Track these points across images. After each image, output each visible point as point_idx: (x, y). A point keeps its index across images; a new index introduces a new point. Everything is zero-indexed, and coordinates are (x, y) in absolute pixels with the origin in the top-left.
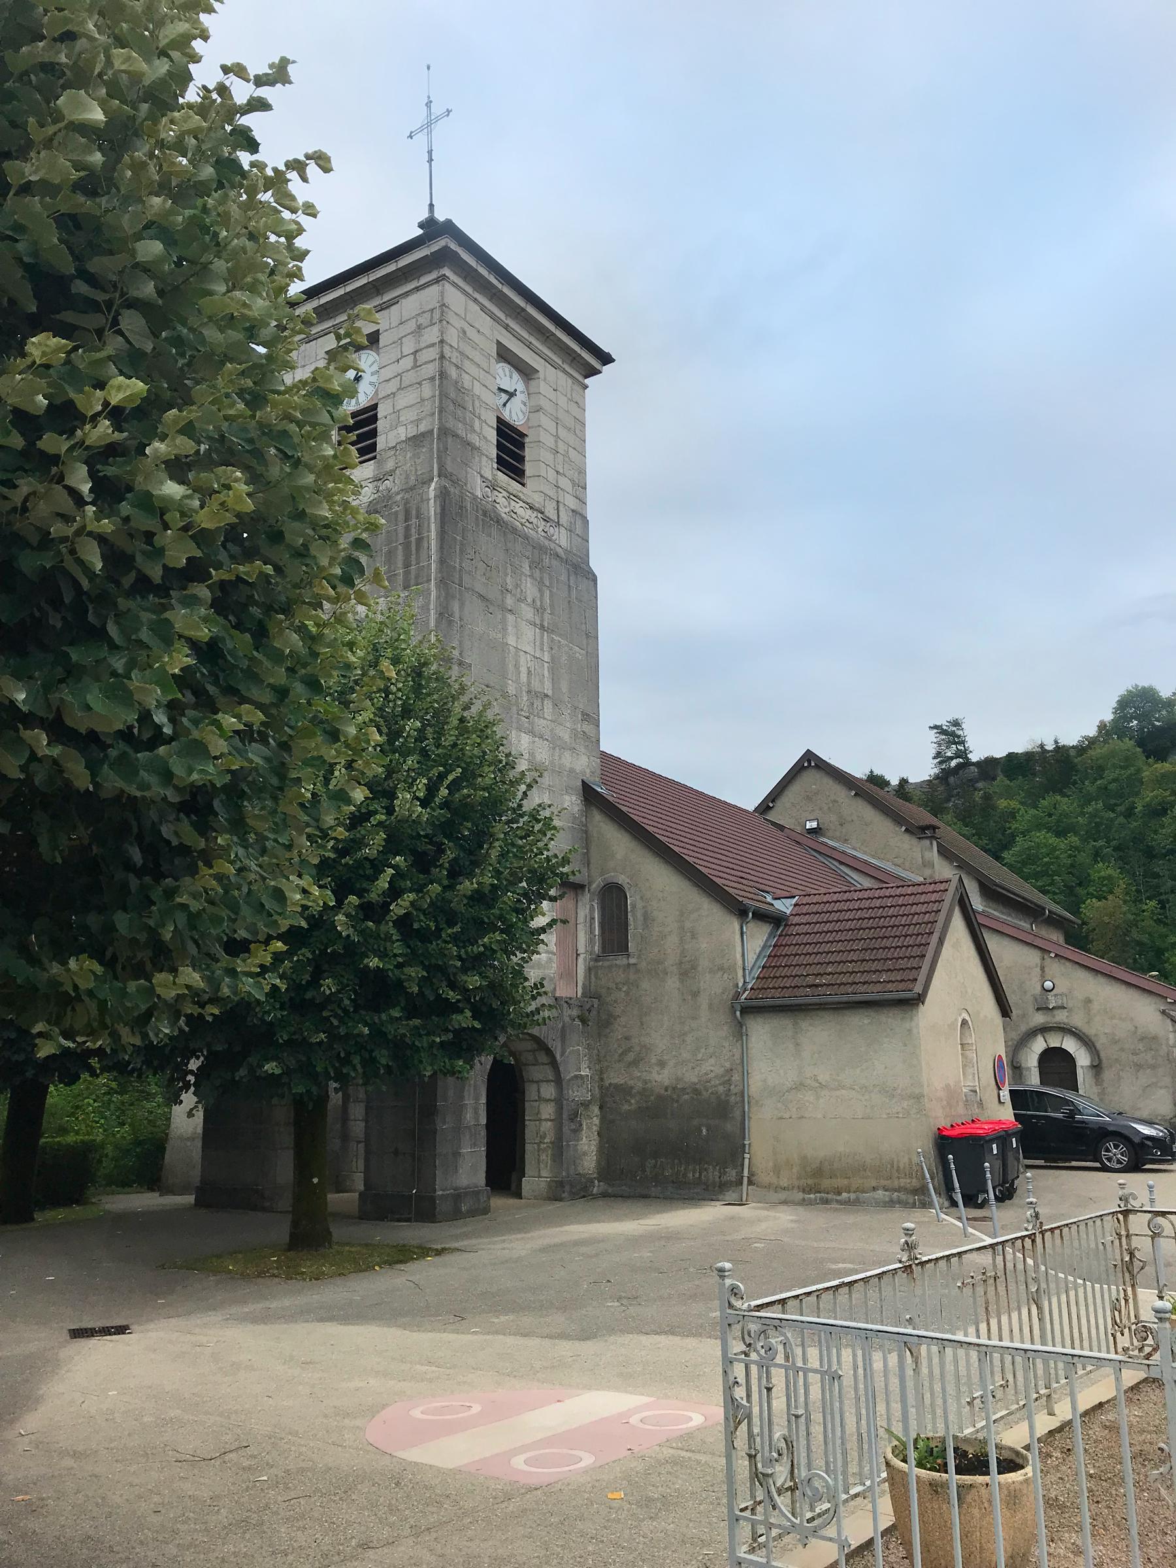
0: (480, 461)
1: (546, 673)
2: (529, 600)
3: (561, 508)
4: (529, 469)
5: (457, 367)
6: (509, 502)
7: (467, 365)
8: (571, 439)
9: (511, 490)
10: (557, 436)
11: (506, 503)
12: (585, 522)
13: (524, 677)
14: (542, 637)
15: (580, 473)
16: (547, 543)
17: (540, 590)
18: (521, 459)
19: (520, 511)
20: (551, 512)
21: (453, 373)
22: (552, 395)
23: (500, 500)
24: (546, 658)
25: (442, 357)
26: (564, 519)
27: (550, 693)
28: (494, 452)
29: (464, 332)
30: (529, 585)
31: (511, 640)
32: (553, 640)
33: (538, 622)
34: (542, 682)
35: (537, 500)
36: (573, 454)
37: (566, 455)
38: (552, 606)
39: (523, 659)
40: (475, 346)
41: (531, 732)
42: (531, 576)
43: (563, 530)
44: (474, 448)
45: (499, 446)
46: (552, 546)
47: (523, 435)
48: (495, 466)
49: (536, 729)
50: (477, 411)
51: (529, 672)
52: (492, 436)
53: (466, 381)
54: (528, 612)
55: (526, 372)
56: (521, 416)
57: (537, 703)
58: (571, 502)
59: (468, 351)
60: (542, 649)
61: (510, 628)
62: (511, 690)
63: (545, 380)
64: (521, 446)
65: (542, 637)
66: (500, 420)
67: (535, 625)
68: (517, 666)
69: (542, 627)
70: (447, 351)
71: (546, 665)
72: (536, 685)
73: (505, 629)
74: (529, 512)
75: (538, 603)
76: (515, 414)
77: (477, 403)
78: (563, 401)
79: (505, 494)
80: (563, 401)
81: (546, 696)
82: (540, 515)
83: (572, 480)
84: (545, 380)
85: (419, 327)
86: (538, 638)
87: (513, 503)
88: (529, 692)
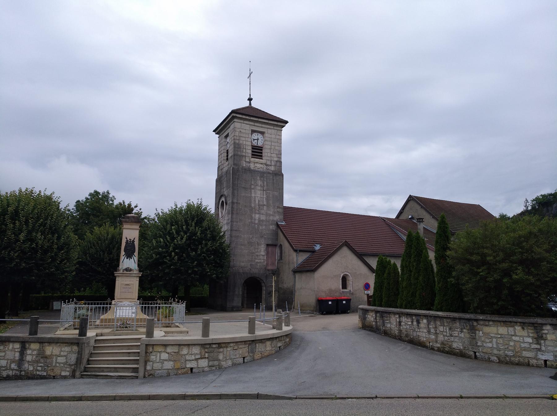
7: (242, 138)
8: (276, 144)
13: (257, 202)
20: (269, 163)
21: (237, 141)
24: (265, 196)
42: (260, 180)
44: (243, 156)
53: (241, 142)
54: (259, 188)
55: (262, 133)
57: (261, 207)
58: (276, 159)
59: (242, 135)
62: (253, 205)
68: (255, 201)
69: (264, 190)
70: (235, 137)
73: (251, 193)
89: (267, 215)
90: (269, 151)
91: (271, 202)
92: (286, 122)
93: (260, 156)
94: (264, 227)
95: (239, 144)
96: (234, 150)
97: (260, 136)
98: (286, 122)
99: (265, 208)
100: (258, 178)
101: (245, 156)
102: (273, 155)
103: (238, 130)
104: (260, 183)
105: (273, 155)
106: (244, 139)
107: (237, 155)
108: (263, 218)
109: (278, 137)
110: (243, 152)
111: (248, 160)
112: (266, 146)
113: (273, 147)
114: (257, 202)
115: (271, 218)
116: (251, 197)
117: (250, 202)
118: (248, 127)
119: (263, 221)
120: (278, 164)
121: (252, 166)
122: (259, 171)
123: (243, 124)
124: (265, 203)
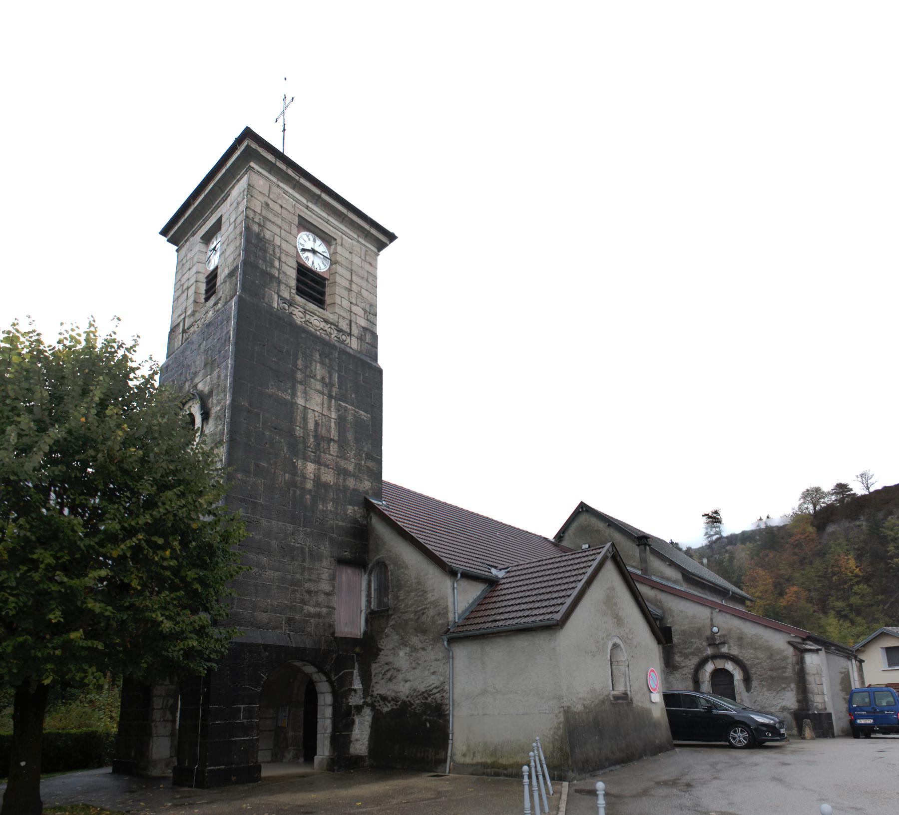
0: (279, 286)
1: (333, 425)
2: (318, 377)
3: (353, 324)
4: (328, 300)
5: (259, 225)
6: (304, 314)
7: (269, 225)
8: (364, 284)
9: (307, 308)
10: (351, 281)
11: (302, 315)
12: (375, 337)
13: (311, 425)
14: (330, 402)
15: (371, 305)
16: (337, 344)
17: (329, 372)
18: (323, 294)
19: (316, 323)
20: (344, 325)
21: (256, 228)
22: (348, 255)
23: (296, 312)
24: (333, 415)
25: (247, 217)
26: (355, 331)
27: (336, 438)
28: (293, 283)
29: (267, 205)
30: (318, 367)
31: (300, 401)
32: (340, 405)
33: (326, 392)
34: (329, 431)
35: (332, 317)
37: (359, 294)
38: (340, 383)
39: (310, 415)
40: (277, 215)
41: (318, 461)
42: (322, 363)
43: (354, 339)
44: (272, 277)
45: (298, 280)
46: (343, 346)
47: (325, 279)
48: (294, 291)
49: (322, 461)
51: (316, 424)
52: (293, 273)
53: (268, 235)
54: (319, 386)
55: (327, 239)
56: (322, 266)
57: (324, 445)
58: (363, 323)
59: (271, 216)
60: (329, 409)
61: (299, 394)
62: (299, 432)
63: (342, 245)
64: (324, 286)
65: (330, 402)
66: (298, 263)
67: (322, 393)
68: (305, 419)
69: (330, 397)
70: (251, 215)
72: (323, 431)
73: (294, 394)
75: (327, 380)
76: (319, 265)
77: (277, 250)
78: (357, 260)
80: (357, 260)
81: (333, 440)
83: (364, 309)
84: (342, 245)
85: (238, 204)
86: (326, 402)
87: (308, 317)
89: (341, 472)
90: (345, 293)
91: (350, 436)
92: (392, 237)
93: (320, 302)
94: (330, 506)
95: (260, 238)
96: (245, 250)
97: (320, 247)
98: (392, 237)
99: (334, 448)
100: (317, 356)
101: (279, 282)
102: (355, 309)
103: (263, 199)
104: (319, 371)
106: (276, 230)
107: (255, 267)
108: (328, 477)
109: (367, 267)
110: (272, 266)
111: (286, 295)
112: (338, 279)
113: (354, 287)
114: (311, 425)
115: (351, 483)
116: (293, 405)
117: (292, 421)
118: (288, 203)
119: (326, 486)
120: (368, 338)
121: (298, 316)
122: (317, 337)
123: (275, 190)
124: (334, 434)
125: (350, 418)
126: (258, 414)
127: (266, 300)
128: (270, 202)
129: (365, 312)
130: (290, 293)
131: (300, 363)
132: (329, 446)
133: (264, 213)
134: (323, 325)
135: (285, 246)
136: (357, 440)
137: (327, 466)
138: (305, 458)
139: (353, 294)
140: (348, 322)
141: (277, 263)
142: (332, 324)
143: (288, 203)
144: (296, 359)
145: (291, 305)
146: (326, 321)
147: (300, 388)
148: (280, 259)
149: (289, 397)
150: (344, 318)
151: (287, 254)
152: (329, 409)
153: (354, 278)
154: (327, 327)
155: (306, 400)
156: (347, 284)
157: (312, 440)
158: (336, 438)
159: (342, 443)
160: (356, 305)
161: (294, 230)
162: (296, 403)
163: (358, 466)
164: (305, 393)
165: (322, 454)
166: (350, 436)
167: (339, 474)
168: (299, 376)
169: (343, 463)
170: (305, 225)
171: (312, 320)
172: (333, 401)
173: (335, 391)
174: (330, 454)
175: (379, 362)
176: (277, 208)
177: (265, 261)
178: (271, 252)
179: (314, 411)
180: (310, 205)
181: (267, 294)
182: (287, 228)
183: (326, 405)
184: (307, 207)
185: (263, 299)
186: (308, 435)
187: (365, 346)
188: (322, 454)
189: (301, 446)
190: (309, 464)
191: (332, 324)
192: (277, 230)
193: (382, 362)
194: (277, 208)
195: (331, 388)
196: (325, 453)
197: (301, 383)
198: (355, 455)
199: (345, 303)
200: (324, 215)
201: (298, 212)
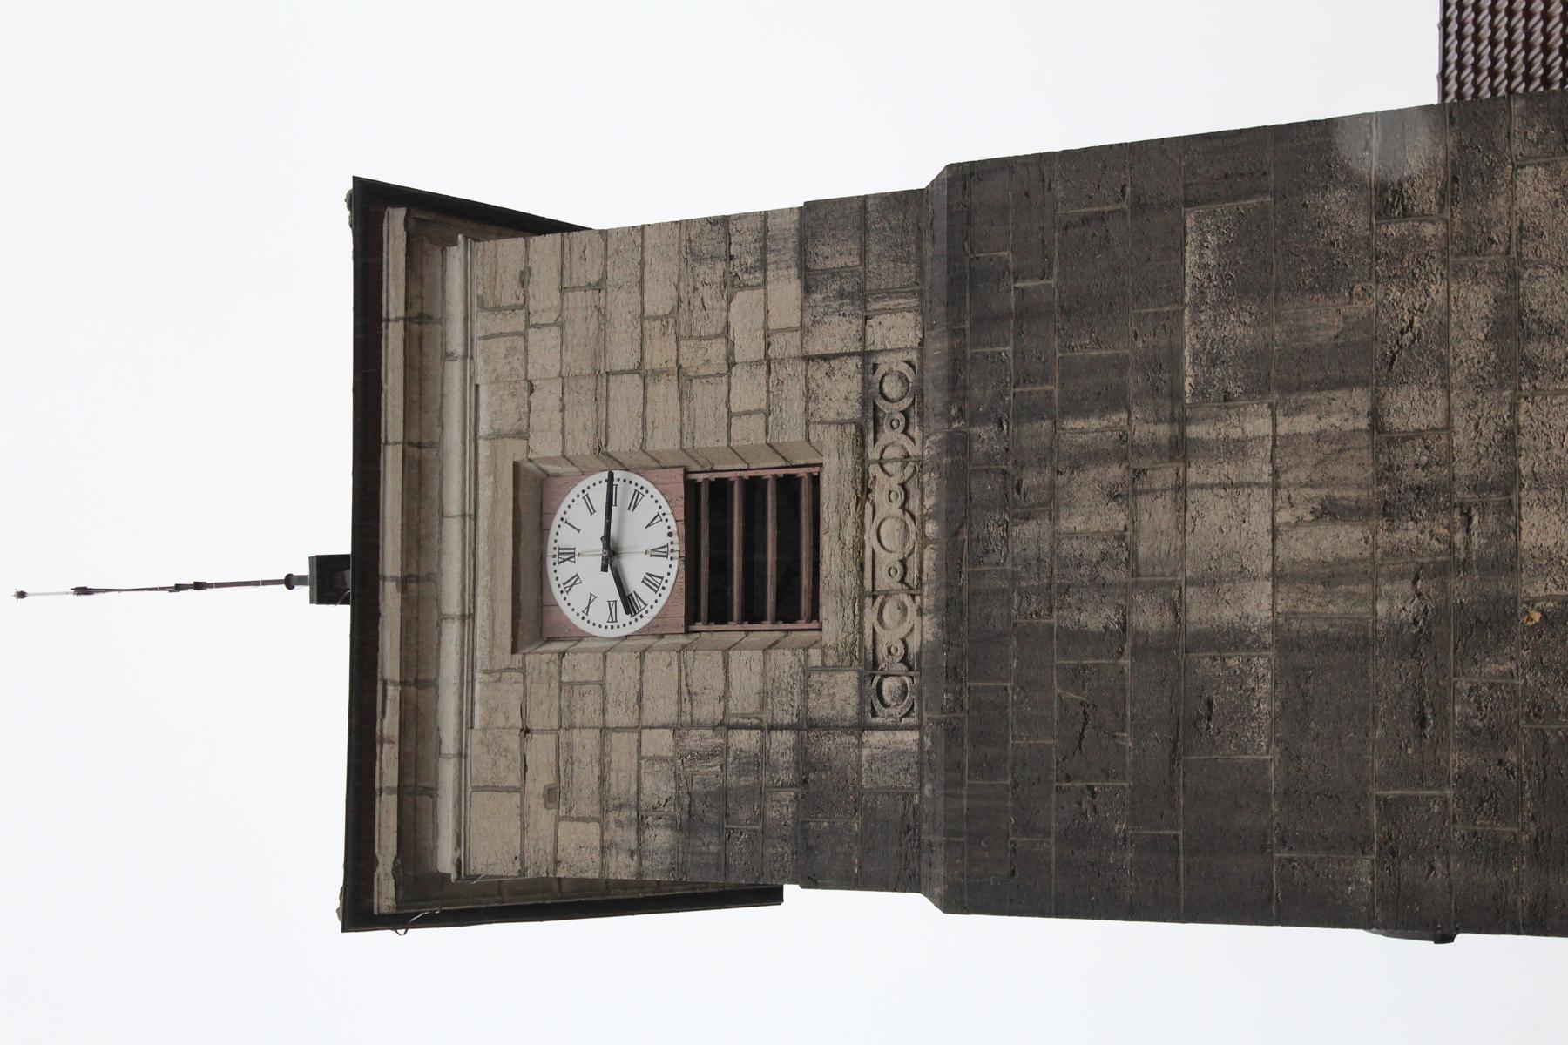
0: (827, 726)
1: (1305, 424)
3: (816, 348)
13: (1345, 540)
23: (890, 638)
24: (1258, 424)
32: (1201, 392)
34: (1340, 443)
36: (659, 299)
50: (711, 739)
51: (1328, 512)
54: (1157, 514)
57: (1413, 464)
61: (1228, 614)
62: (1396, 604)
68: (1330, 575)
71: (1284, 427)
72: (1353, 476)
74: (879, 496)
79: (870, 617)
82: (873, 453)
88: (1389, 511)
90: (706, 397)
91: (1325, 320)
99: (1412, 408)
102: (748, 346)
105: (748, 346)
110: (760, 761)
113: (660, 354)
116: (1288, 642)
120: (836, 255)
124: (1344, 412)
125: (1239, 330)
126: (1387, 805)
127: (908, 781)
128: (541, 779)
129: (731, 286)
130: (824, 668)
131: (1096, 618)
132: (1407, 437)
133: (587, 807)
134: (886, 504)
135: (662, 707)
136: (1330, 280)
137: (1511, 435)
138: (1509, 562)
139: (691, 357)
140: (818, 372)
141: (744, 740)
142: (862, 457)
143: (497, 702)
144: (1078, 637)
145: (871, 668)
146: (864, 489)
147: (1200, 612)
148: (725, 726)
149: (1262, 665)
150: (809, 396)
151: (685, 693)
152: (1237, 449)
153: (622, 355)
154: (885, 485)
155: (1242, 574)
156: (664, 392)
157: (1408, 533)
158: (1360, 398)
159: (1373, 362)
160: (726, 332)
161: (581, 666)
162: (1275, 627)
163: (1464, 251)
164: (1210, 581)
165: (1462, 470)
166: (1325, 320)
167: (1532, 367)
168: (1150, 618)
169: (1470, 347)
170: (534, 618)
171: (888, 560)
172: (1194, 431)
173: (1150, 430)
174: (1448, 427)
175: (922, 182)
176: (542, 749)
177: (758, 794)
178: (714, 766)
179: (1274, 532)
180: (452, 605)
181: (885, 781)
182: (591, 700)
183: (1229, 470)
184: (468, 617)
185: (907, 796)
186: (1394, 552)
187: (882, 271)
188: (1462, 470)
189: (1462, 588)
190: (1528, 539)
191: (862, 457)
192: (622, 745)
193: (919, 176)
194: (542, 749)
195: (1140, 450)
196: (1448, 458)
197: (1177, 608)
198: (1409, 281)
199: (747, 391)
200: (453, 531)
201: (504, 656)
